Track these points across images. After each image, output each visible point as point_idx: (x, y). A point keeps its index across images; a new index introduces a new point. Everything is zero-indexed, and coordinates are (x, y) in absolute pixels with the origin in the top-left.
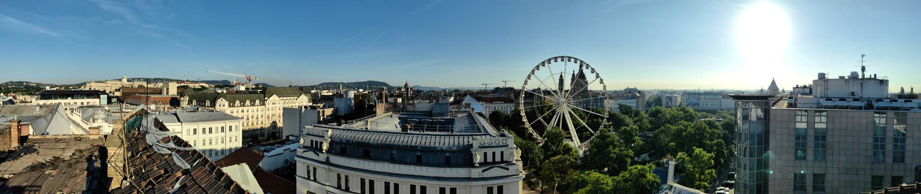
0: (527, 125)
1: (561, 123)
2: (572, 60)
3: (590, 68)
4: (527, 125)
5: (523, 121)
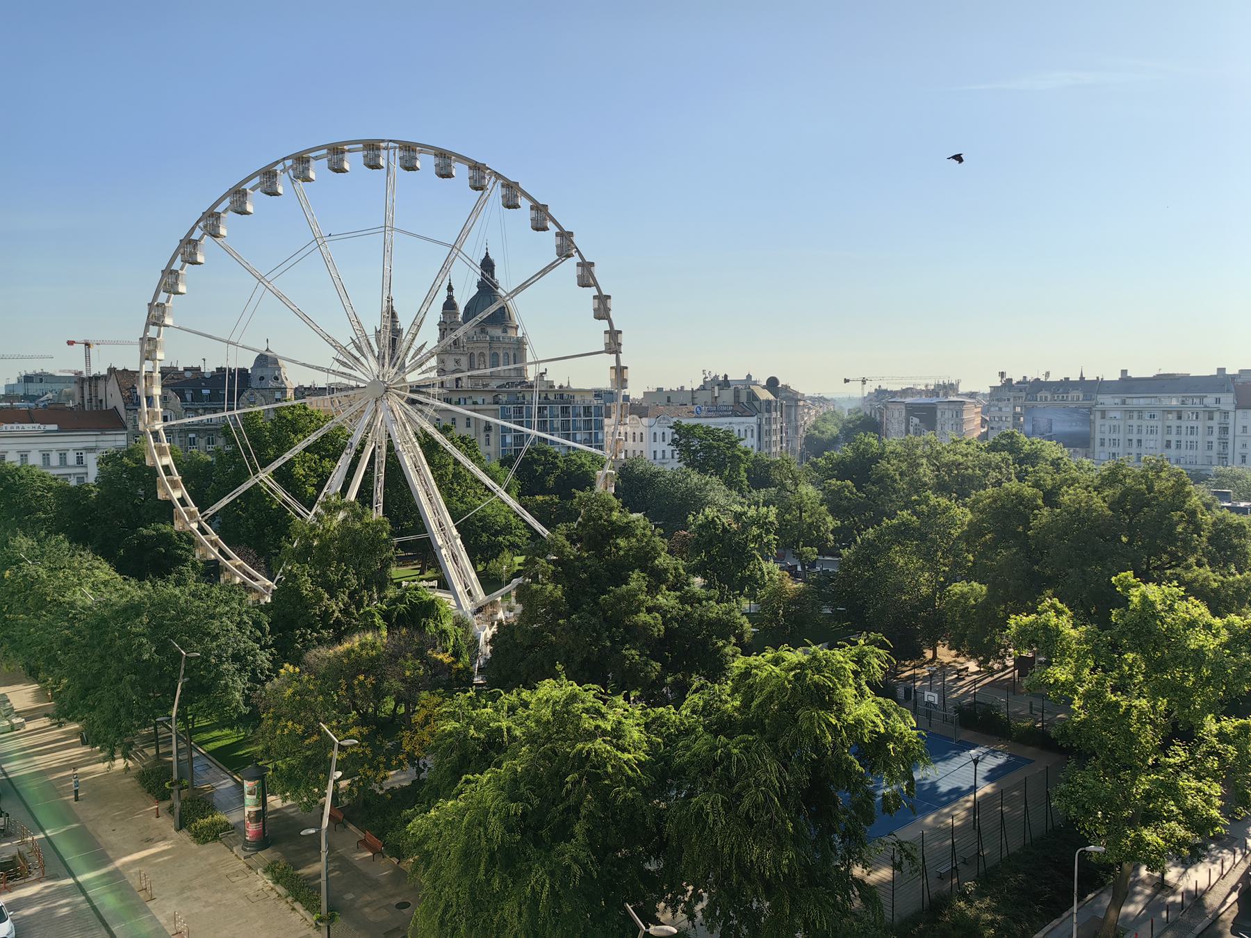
0: (189, 519)
1: (379, 495)
2: (426, 162)
3: (522, 201)
4: (189, 519)
5: (161, 495)
